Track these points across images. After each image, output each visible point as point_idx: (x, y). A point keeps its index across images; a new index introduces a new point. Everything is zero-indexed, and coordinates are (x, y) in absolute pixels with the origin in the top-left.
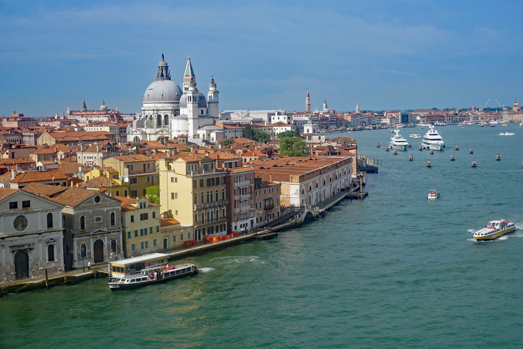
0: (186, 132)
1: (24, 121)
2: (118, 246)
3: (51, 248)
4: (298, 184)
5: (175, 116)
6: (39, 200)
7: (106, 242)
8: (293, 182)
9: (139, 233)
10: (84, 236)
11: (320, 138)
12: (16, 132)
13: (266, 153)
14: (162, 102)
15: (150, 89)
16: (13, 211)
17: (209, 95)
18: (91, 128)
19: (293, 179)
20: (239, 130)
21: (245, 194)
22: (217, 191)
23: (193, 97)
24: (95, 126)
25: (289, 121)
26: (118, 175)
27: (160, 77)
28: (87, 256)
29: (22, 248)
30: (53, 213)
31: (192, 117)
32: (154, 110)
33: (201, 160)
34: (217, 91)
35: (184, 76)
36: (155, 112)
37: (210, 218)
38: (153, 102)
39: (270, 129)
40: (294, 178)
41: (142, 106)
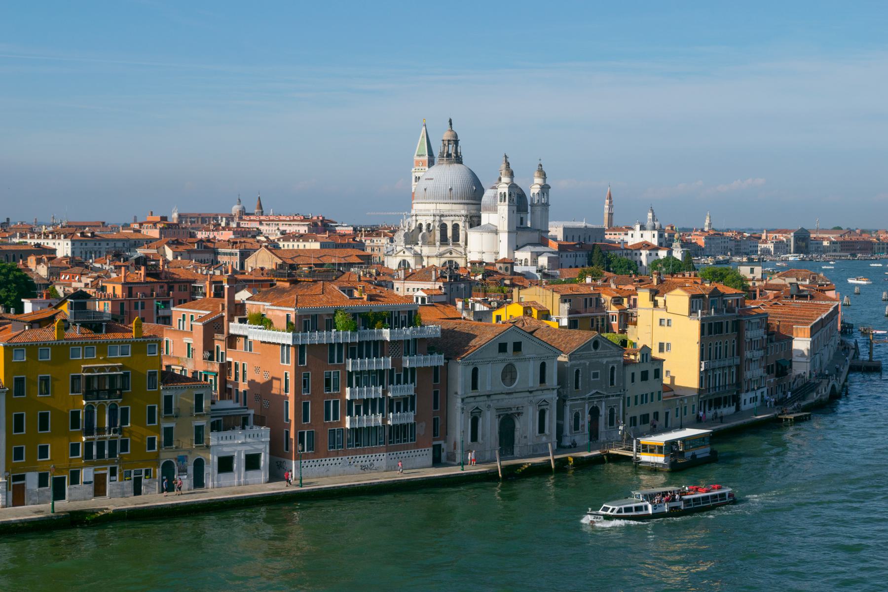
2: (617, 417)
3: (542, 414)
6: (533, 342)
7: (603, 411)
11: (752, 271)
15: (428, 179)
16: (502, 356)
19: (799, 331)
23: (510, 195)
24: (294, 241)
28: (580, 430)
29: (510, 412)
31: (506, 229)
33: (708, 293)
37: (717, 385)
38: (433, 201)
39: (628, 255)
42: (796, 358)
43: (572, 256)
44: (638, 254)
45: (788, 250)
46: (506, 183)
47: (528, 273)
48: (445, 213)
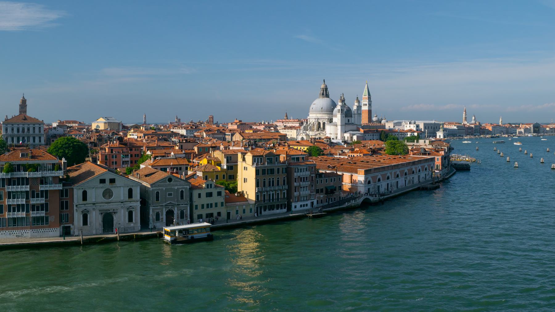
1: (241, 125)
2: (186, 215)
5: (330, 123)
7: (176, 212)
9: (205, 206)
10: (158, 206)
12: (221, 132)
13: (370, 152)
16: (102, 185)
18: (285, 130)
19: (360, 172)
21: (306, 182)
22: (278, 178)
23: (341, 110)
25: (418, 128)
26: (221, 164)
28: (160, 220)
29: (109, 212)
30: (133, 188)
31: (340, 124)
35: (363, 96)
37: (271, 198)
39: (402, 134)
41: (309, 116)
43: (371, 135)
44: (407, 134)
45: (531, 132)
46: (340, 105)
47: (339, 142)
48: (319, 118)
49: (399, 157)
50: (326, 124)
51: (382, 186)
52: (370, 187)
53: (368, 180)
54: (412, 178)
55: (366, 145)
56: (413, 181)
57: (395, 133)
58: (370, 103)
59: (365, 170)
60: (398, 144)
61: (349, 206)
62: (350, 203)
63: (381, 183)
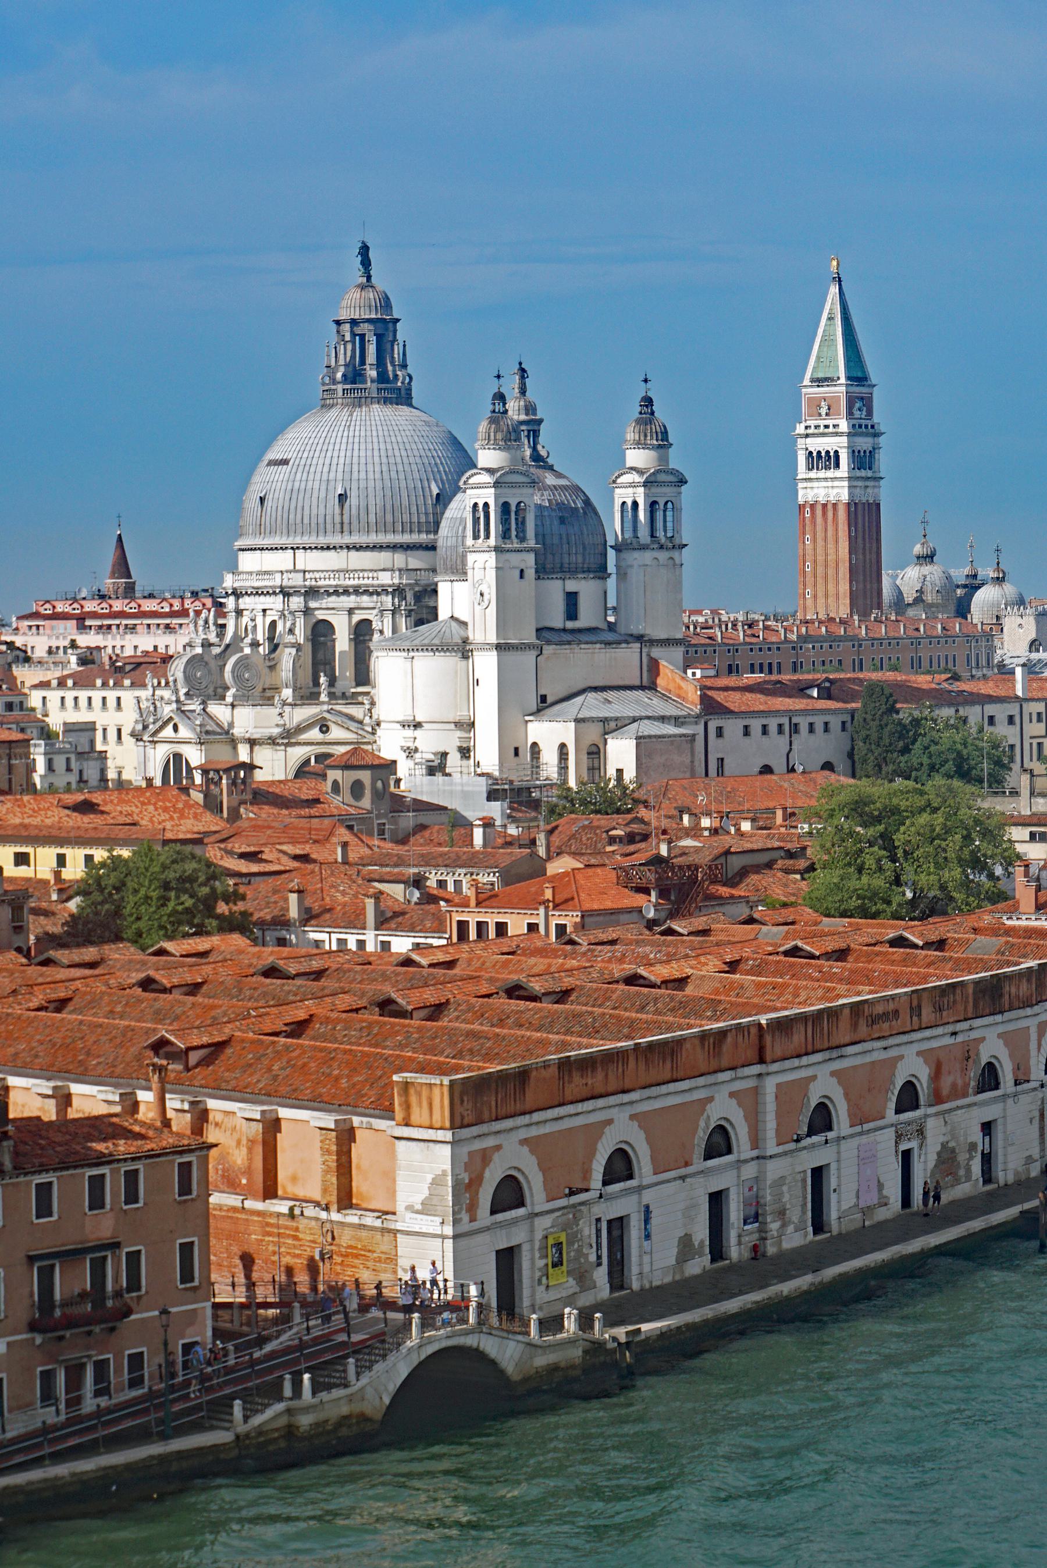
0: (459, 734)
4: (440, 1135)
5: (420, 622)
8: (415, 1118)
13: (647, 891)
14: (337, 539)
17: (623, 495)
18: (83, 695)
19: (413, 1099)
20: (819, 721)
23: (505, 508)
24: (105, 684)
27: (340, 388)
31: (493, 639)
32: (285, 592)
34: (674, 472)
35: (806, 382)
36: (297, 602)
40: (419, 1094)
41: (233, 568)
42: (409, 1215)
43: (773, 729)
46: (490, 471)
49: (892, 935)
50: (376, 636)
51: (647, 1220)
52: (517, 1237)
53: (492, 1177)
54: (977, 1136)
55: (686, 818)
56: (987, 1159)
57: (990, 709)
58: (864, 443)
59: (452, 1083)
60: (922, 810)
61: (260, 1431)
62: (280, 1407)
63: (640, 1189)
